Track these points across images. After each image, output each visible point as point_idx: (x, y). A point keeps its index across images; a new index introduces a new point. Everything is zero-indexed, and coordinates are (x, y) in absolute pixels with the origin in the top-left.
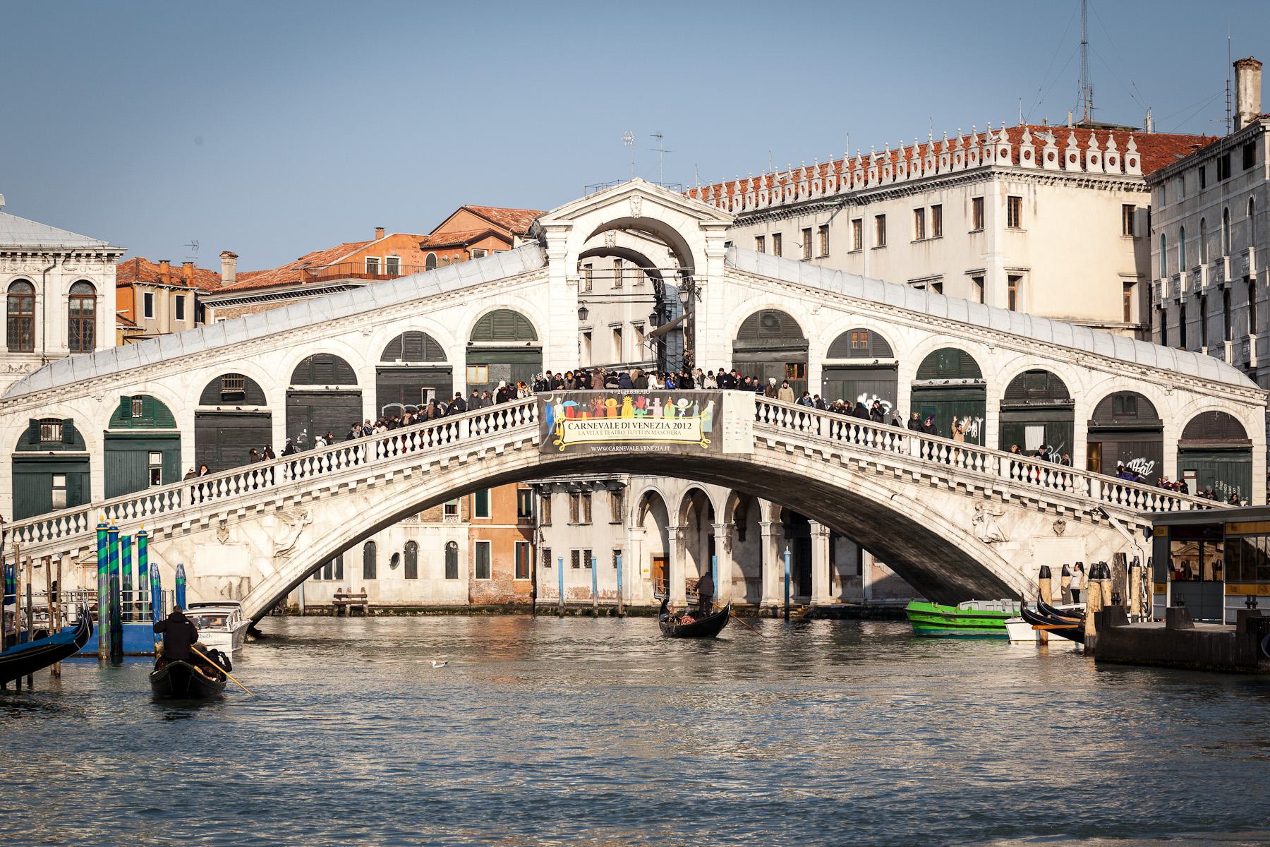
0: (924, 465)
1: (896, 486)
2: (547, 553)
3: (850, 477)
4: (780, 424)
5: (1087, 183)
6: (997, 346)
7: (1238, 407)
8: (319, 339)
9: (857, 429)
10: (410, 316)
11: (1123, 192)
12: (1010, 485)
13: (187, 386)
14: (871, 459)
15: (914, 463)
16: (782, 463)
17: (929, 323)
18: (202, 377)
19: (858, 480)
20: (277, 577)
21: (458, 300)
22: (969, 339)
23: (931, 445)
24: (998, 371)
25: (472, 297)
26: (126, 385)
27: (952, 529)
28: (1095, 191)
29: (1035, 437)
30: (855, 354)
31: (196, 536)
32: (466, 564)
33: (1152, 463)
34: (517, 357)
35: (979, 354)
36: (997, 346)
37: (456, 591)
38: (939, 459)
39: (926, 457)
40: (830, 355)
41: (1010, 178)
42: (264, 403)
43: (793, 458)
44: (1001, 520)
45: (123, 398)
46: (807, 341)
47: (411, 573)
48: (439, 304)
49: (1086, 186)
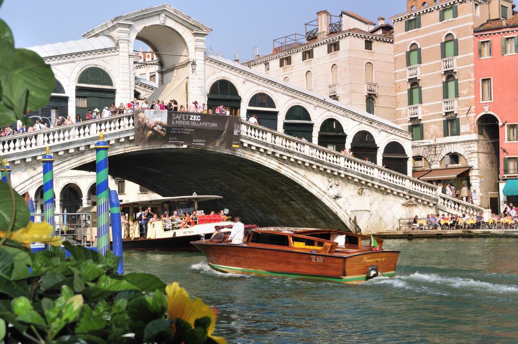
1: (296, 169)
6: (317, 106)
14: (289, 155)
16: (247, 156)
17: (291, 93)
19: (281, 166)
21: (72, 59)
24: (318, 117)
27: (319, 191)
34: (102, 94)
35: (310, 109)
36: (317, 106)
40: (250, 105)
44: (338, 187)
46: (240, 97)
48: (61, 61)
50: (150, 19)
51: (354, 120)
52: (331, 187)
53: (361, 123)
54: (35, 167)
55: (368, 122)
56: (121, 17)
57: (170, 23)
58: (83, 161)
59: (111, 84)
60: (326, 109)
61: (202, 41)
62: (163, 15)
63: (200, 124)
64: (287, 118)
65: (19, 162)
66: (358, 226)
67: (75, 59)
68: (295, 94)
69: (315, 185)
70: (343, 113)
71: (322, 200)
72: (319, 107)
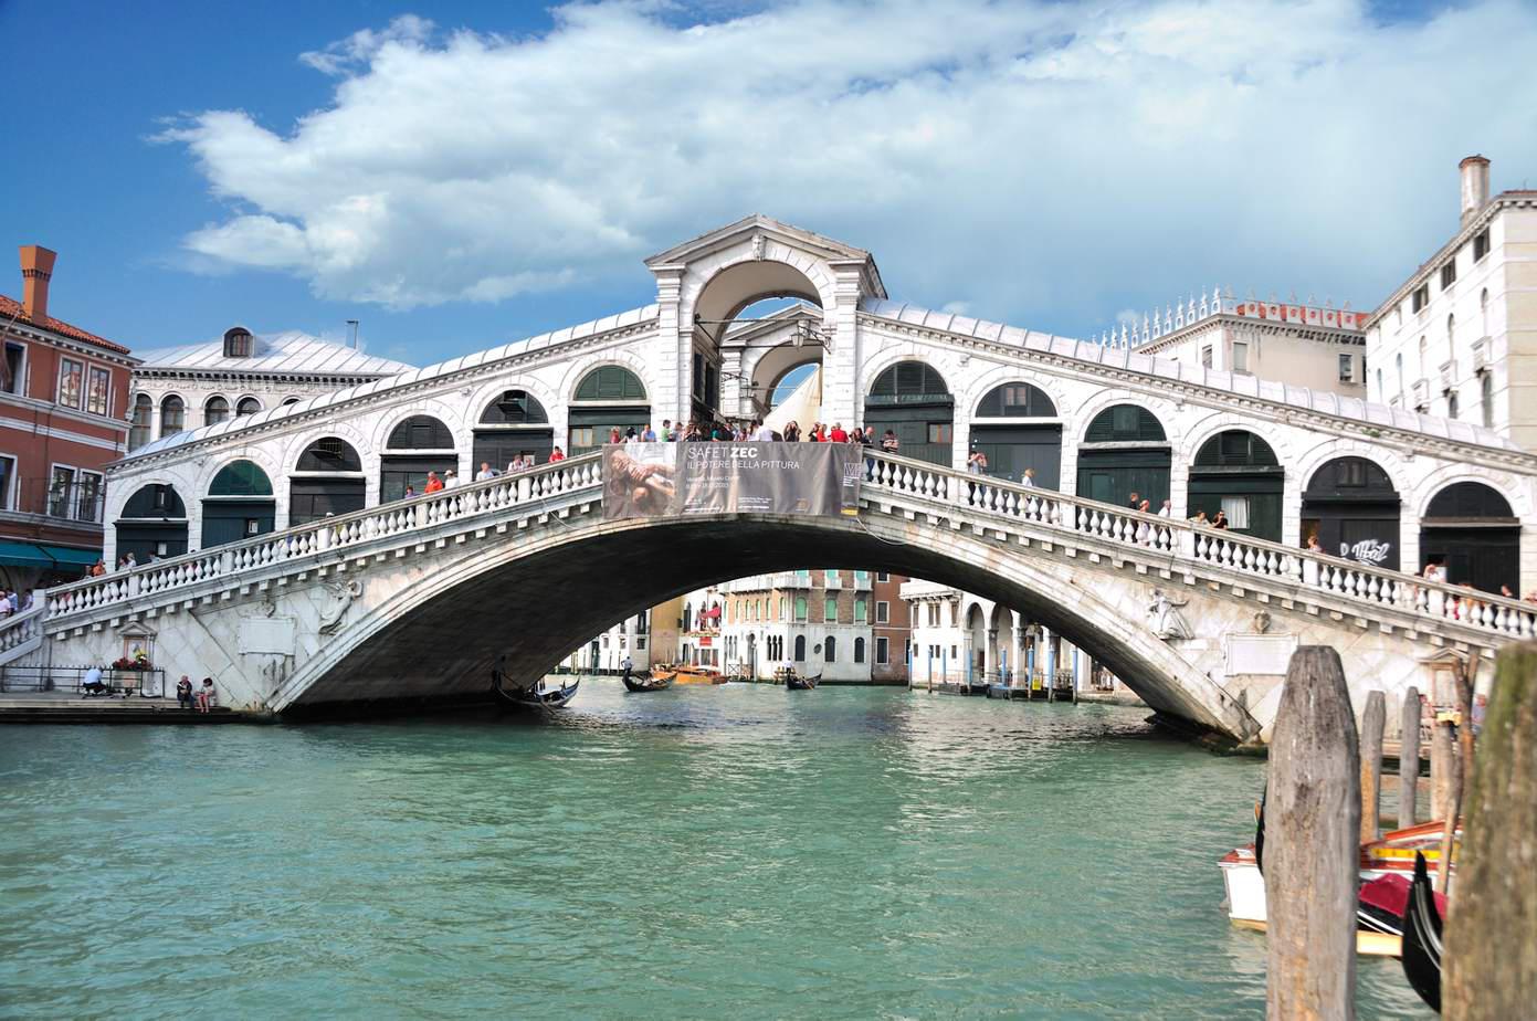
0: (1079, 538)
1: (1045, 565)
2: (916, 646)
4: (897, 485)
5: (1306, 334)
6: (1184, 401)
7: (1502, 476)
8: (417, 399)
9: (994, 493)
10: (510, 374)
11: (1340, 345)
12: (1194, 565)
13: (284, 452)
14: (1010, 530)
16: (901, 534)
17: (1103, 374)
18: (301, 440)
19: (996, 557)
20: (322, 656)
22: (1150, 394)
24: (1186, 432)
25: (580, 352)
26: (226, 449)
27: (1117, 620)
28: (1314, 342)
29: (1237, 512)
30: (1011, 411)
31: (243, 609)
32: (869, 653)
33: (1386, 546)
35: (1162, 411)
36: (1184, 401)
37: (863, 671)
38: (1100, 531)
39: (1082, 528)
40: (979, 413)
41: (1235, 327)
42: (359, 470)
43: (915, 529)
44: (1183, 611)
46: (952, 396)
47: (830, 657)
49: (1306, 337)
50: (731, 251)
51: (1315, 431)
52: (1154, 609)
53: (1341, 437)
54: (421, 566)
55: (1365, 433)
56: (655, 257)
57: (778, 253)
58: (512, 553)
59: (642, 394)
60: (1215, 408)
61: (849, 281)
62: (756, 240)
63: (757, 464)
64: (1089, 437)
65: (383, 558)
66: (1247, 713)
67: (571, 354)
68: (1113, 377)
69: (1103, 605)
70: (1276, 415)
71: (1129, 644)
72: (1192, 403)
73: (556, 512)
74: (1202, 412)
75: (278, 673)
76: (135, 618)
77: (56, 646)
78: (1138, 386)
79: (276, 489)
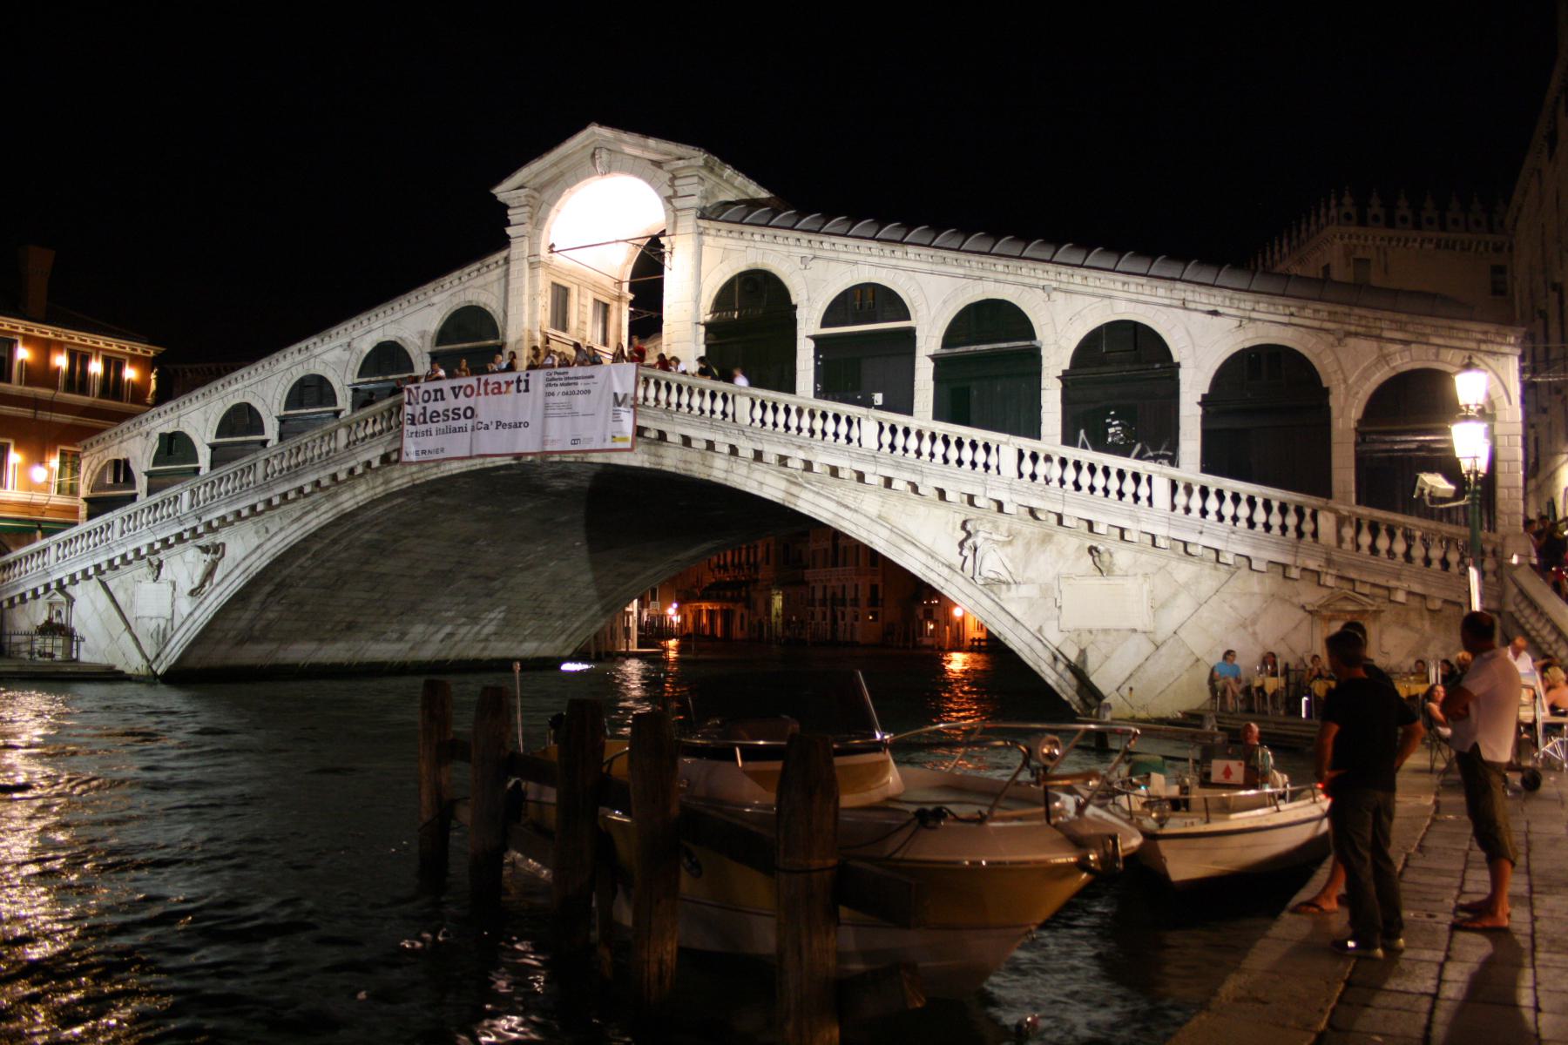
3: (783, 485)
12: (1011, 489)
13: (207, 420)
14: (802, 455)
15: (862, 458)
19: (794, 490)
20: (191, 620)
23: (893, 430)
27: (931, 562)
40: (824, 324)
45: (162, 436)
49: (1447, 246)
51: (1215, 313)
72: (1066, 292)
73: (368, 464)
74: (1079, 302)
75: (163, 639)
76: (54, 586)
77: (8, 613)
78: (1002, 277)
79: (201, 458)
